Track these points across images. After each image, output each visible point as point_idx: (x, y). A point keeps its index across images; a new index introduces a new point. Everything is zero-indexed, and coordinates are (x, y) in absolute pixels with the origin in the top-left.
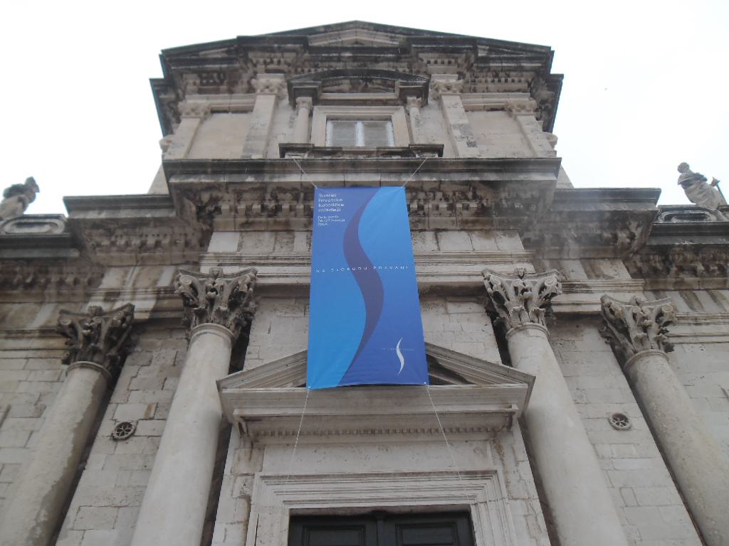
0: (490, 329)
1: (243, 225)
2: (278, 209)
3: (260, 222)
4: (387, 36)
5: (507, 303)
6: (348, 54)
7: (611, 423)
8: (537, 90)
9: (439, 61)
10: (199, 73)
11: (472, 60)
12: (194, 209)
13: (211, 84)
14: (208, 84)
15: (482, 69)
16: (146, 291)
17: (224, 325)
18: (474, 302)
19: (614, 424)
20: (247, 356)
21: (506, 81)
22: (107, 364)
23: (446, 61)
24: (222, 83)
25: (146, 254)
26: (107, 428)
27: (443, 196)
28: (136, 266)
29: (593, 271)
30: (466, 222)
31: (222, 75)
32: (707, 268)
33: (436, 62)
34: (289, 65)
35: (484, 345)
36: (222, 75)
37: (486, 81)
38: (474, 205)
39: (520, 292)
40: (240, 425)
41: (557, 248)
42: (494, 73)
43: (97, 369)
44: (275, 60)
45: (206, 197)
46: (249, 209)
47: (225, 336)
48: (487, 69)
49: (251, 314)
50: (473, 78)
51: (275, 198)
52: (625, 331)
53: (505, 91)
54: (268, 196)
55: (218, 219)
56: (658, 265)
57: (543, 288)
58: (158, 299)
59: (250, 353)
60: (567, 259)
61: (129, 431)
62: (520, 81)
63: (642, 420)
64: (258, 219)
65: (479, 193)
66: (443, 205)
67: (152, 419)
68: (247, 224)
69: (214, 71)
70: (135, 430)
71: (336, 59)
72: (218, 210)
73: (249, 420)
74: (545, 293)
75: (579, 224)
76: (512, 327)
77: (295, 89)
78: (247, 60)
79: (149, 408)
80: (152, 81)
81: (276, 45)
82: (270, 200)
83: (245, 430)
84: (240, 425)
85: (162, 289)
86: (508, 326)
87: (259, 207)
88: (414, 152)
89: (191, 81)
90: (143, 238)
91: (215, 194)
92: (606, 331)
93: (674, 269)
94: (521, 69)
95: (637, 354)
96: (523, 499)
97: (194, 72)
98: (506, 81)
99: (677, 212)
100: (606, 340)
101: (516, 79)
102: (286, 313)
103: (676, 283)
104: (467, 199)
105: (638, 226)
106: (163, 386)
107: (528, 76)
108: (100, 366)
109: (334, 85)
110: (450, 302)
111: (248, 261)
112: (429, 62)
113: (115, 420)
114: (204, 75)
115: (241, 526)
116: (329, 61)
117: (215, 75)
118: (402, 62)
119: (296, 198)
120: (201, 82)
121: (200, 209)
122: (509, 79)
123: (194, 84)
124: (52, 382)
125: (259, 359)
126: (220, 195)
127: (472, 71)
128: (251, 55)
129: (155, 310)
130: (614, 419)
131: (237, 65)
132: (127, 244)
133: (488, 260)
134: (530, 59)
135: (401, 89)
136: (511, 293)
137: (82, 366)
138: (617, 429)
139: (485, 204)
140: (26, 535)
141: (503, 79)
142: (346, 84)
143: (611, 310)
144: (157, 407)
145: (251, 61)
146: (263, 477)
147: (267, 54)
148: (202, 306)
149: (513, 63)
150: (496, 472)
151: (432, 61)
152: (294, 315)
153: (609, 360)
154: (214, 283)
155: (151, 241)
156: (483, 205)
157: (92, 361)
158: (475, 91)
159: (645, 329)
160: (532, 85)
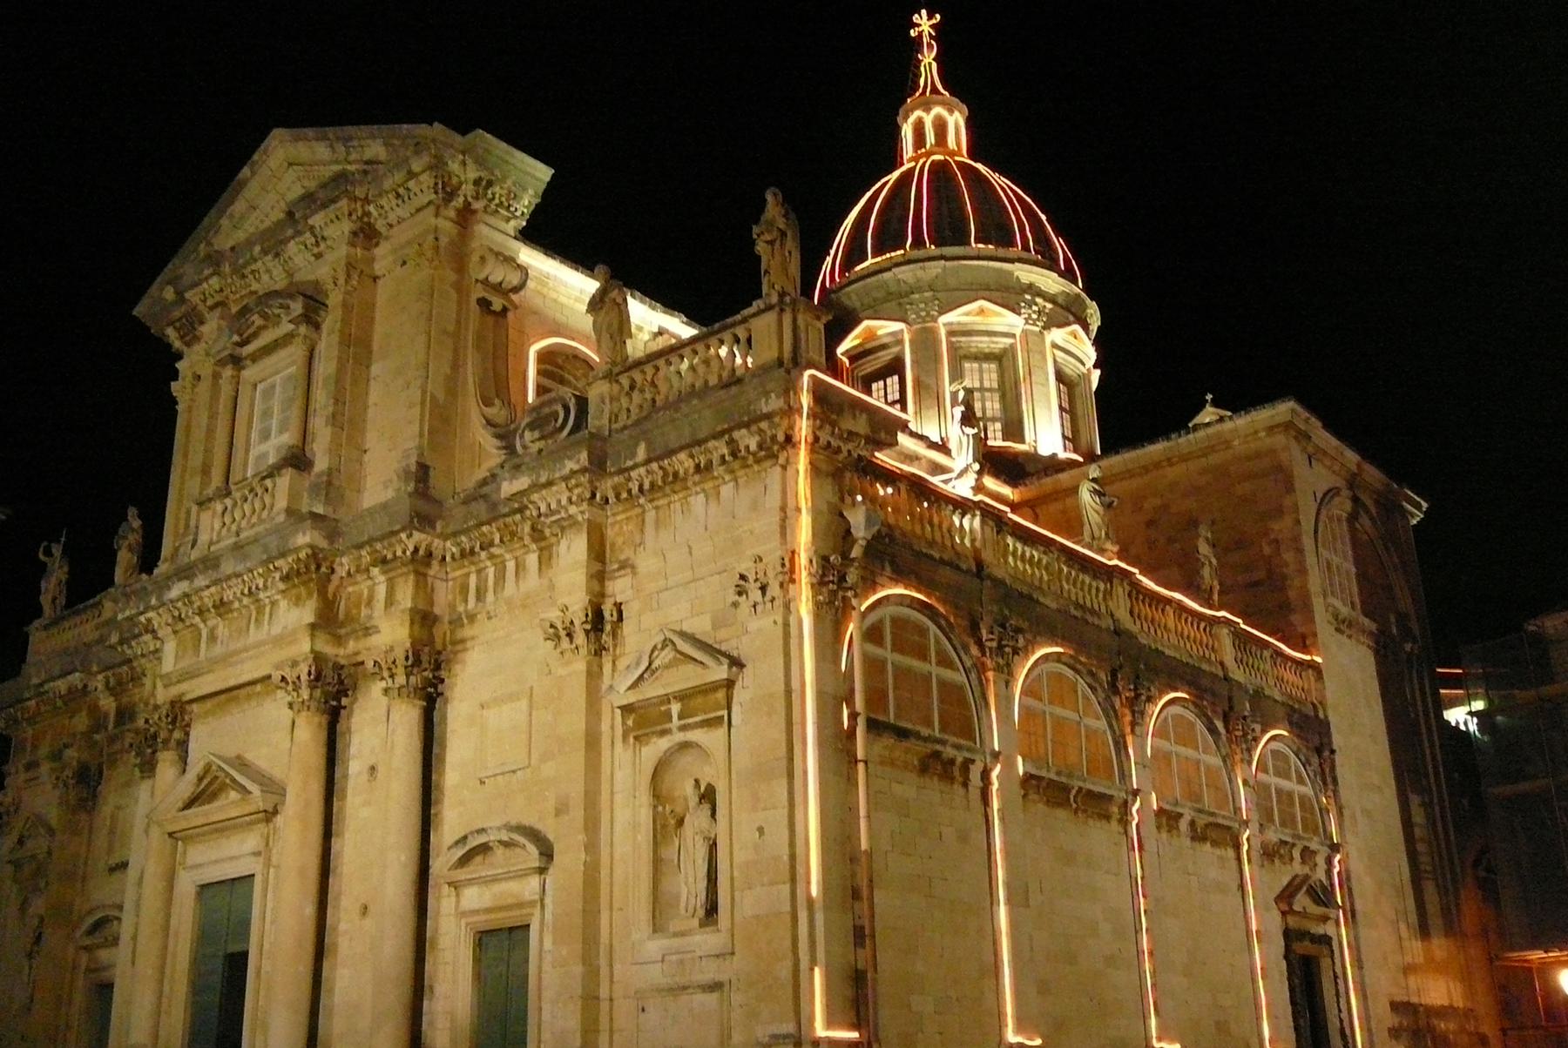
6: (257, 249)
10: (171, 323)
15: (380, 195)
23: (333, 217)
30: (283, 591)
32: (502, 541)
33: (326, 224)
37: (392, 209)
38: (277, 575)
49: (188, 725)
69: (181, 318)
94: (412, 175)
97: (168, 325)
99: (534, 415)
107: (427, 179)
109: (248, 328)
114: (178, 324)
117: (184, 320)
141: (406, 198)
142: (258, 321)
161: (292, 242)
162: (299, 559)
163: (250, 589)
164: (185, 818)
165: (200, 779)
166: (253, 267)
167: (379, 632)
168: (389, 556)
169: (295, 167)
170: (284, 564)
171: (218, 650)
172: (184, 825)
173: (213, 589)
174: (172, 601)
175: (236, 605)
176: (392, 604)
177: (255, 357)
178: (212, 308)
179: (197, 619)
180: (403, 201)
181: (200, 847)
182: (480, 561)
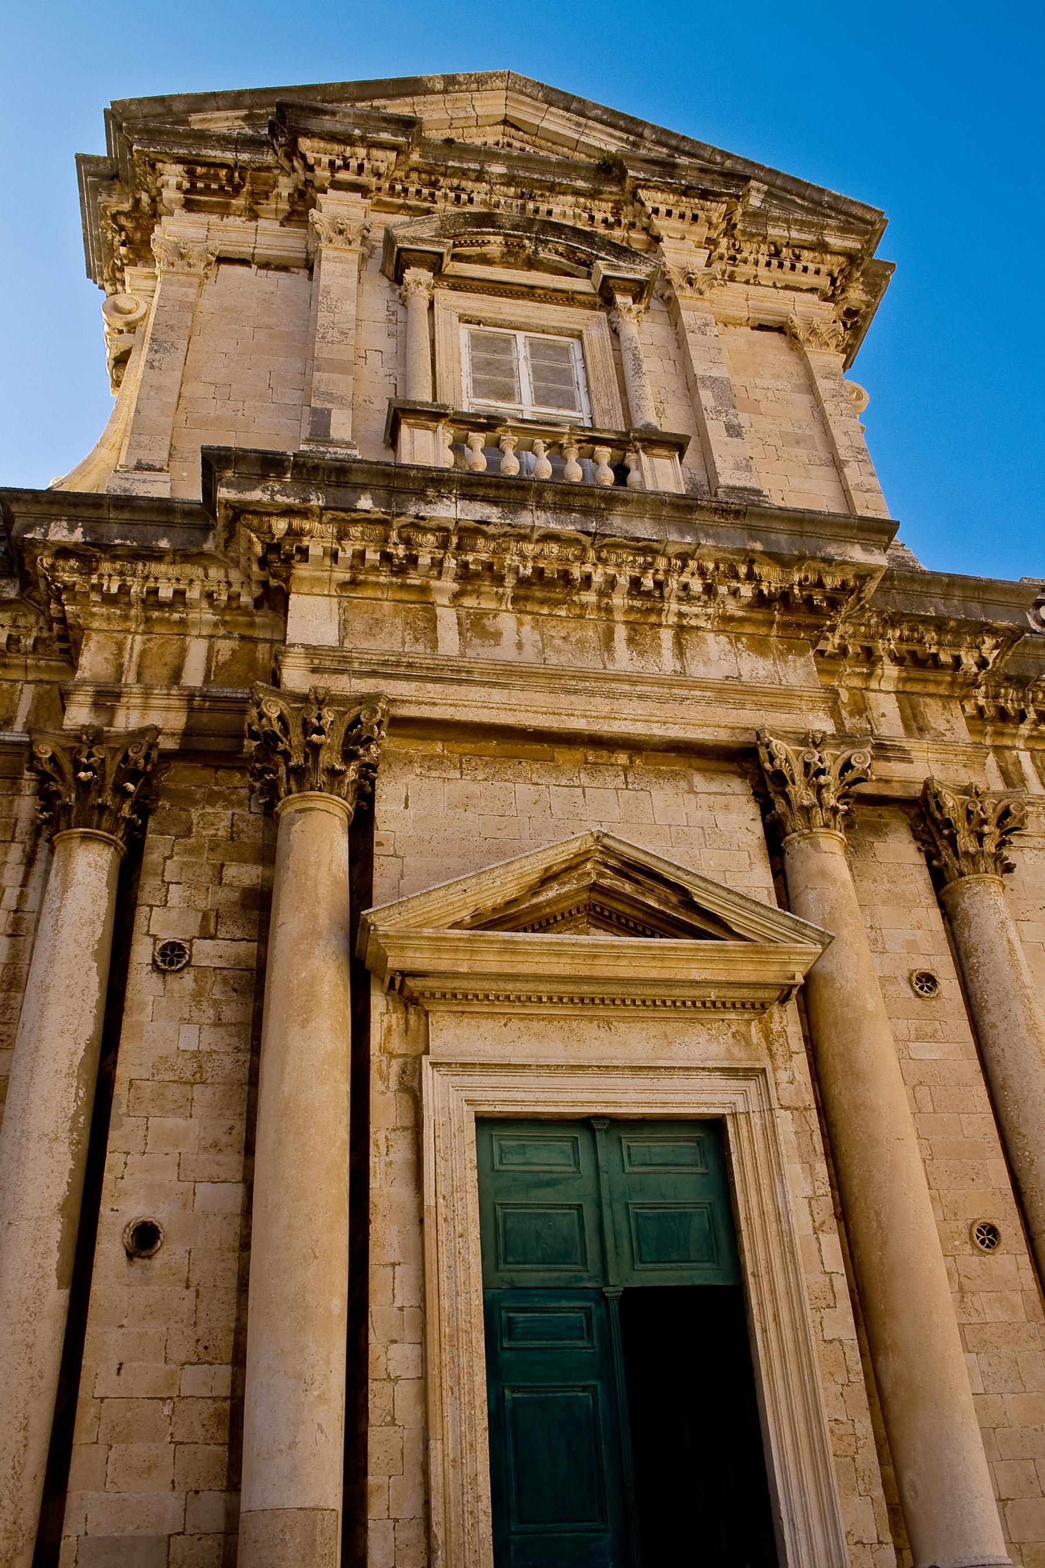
0: (758, 828)
1: (343, 585)
2: (413, 560)
3: (377, 584)
4: (569, 119)
5: (790, 789)
6: (498, 169)
7: (912, 986)
8: (843, 291)
9: (676, 212)
10: (189, 163)
11: (737, 217)
12: (258, 549)
13: (214, 193)
14: (207, 191)
16: (168, 694)
17: (339, 795)
18: (734, 773)
19: (917, 989)
20: (376, 850)
21: (793, 268)
22: (121, 834)
24: (237, 190)
25: (156, 614)
26: (142, 952)
27: (698, 569)
28: (136, 633)
29: (915, 716)
30: (731, 619)
31: (236, 174)
33: (669, 213)
34: (379, 175)
35: (749, 856)
36: (236, 174)
37: (756, 263)
38: (747, 591)
39: (812, 772)
40: (392, 980)
41: (865, 670)
42: (773, 248)
43: (109, 843)
44: (354, 163)
45: (280, 526)
46: (360, 556)
47: (338, 811)
48: (760, 238)
49: (374, 768)
50: (732, 252)
51: (408, 542)
52: (952, 840)
53: (787, 287)
54: (394, 536)
55: (301, 570)
56: (1009, 705)
57: (847, 766)
58: (191, 710)
59: (380, 844)
60: (875, 691)
61: (182, 956)
62: (817, 272)
63: (956, 983)
64: (372, 578)
65: (756, 569)
66: (697, 586)
67: (213, 937)
68: (353, 583)
69: (223, 166)
70: (190, 956)
71: (473, 175)
72: (304, 552)
73: (405, 974)
74: (850, 775)
75: (906, 633)
76: (794, 831)
77: (400, 250)
78: (292, 151)
79: (205, 917)
80: (82, 160)
81: (357, 132)
82: (395, 544)
83: (397, 987)
84: (392, 980)
85: (197, 693)
86: (789, 829)
87: (378, 556)
88: (638, 444)
89: (173, 181)
90: (151, 584)
91: (296, 523)
92: (923, 831)
93: (1032, 715)
94: (822, 247)
95: (963, 879)
96: (797, 1109)
97: (179, 160)
98: (793, 268)
100: (919, 844)
101: (812, 267)
102: (430, 769)
103: (1030, 738)
104: (736, 577)
105: (996, 647)
106: (221, 879)
107: (833, 263)
108: (111, 837)
109: (472, 245)
110: (698, 770)
111: (364, 668)
112: (656, 211)
113: (155, 938)
114: (199, 170)
115: (408, 1134)
116: (460, 178)
117: (223, 173)
118: (600, 200)
119: (444, 545)
120: (193, 185)
121: (272, 548)
122: (799, 266)
123: (179, 187)
124: (5, 841)
125: (395, 855)
126: (307, 525)
127: (733, 235)
128: (305, 144)
129: (188, 733)
130: (918, 979)
131: (269, 159)
132: (124, 589)
133: (765, 700)
134: (845, 230)
135: (606, 278)
136: (798, 769)
137: (86, 838)
138: (918, 995)
139: (766, 592)
140: (68, 1125)
141: (787, 264)
142: (495, 245)
143: (937, 803)
144: (217, 917)
145: (303, 157)
146: (434, 1065)
147: (337, 148)
148: (297, 760)
149: (810, 232)
150: (764, 1070)
151: (663, 209)
152: (445, 775)
153: (920, 882)
154: (319, 718)
155: (166, 592)
156: (761, 591)
157: (98, 828)
158: (732, 278)
159: (980, 837)
160: (838, 283)
161: (570, 199)
162: (820, 584)
163: (659, 585)
164: (510, 948)
165: (548, 879)
166: (468, 185)
167: (912, 762)
168: (945, 657)
169: (508, 129)
170: (772, 578)
171: (482, 653)
172: (491, 962)
173: (555, 548)
174: (419, 525)
175: (590, 597)
176: (921, 730)
177: (460, 284)
178: (337, 185)
179: (448, 584)
180: (781, 265)
181: (488, 1025)
182: (1014, 736)
